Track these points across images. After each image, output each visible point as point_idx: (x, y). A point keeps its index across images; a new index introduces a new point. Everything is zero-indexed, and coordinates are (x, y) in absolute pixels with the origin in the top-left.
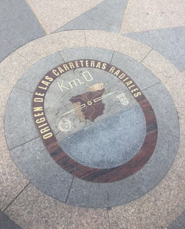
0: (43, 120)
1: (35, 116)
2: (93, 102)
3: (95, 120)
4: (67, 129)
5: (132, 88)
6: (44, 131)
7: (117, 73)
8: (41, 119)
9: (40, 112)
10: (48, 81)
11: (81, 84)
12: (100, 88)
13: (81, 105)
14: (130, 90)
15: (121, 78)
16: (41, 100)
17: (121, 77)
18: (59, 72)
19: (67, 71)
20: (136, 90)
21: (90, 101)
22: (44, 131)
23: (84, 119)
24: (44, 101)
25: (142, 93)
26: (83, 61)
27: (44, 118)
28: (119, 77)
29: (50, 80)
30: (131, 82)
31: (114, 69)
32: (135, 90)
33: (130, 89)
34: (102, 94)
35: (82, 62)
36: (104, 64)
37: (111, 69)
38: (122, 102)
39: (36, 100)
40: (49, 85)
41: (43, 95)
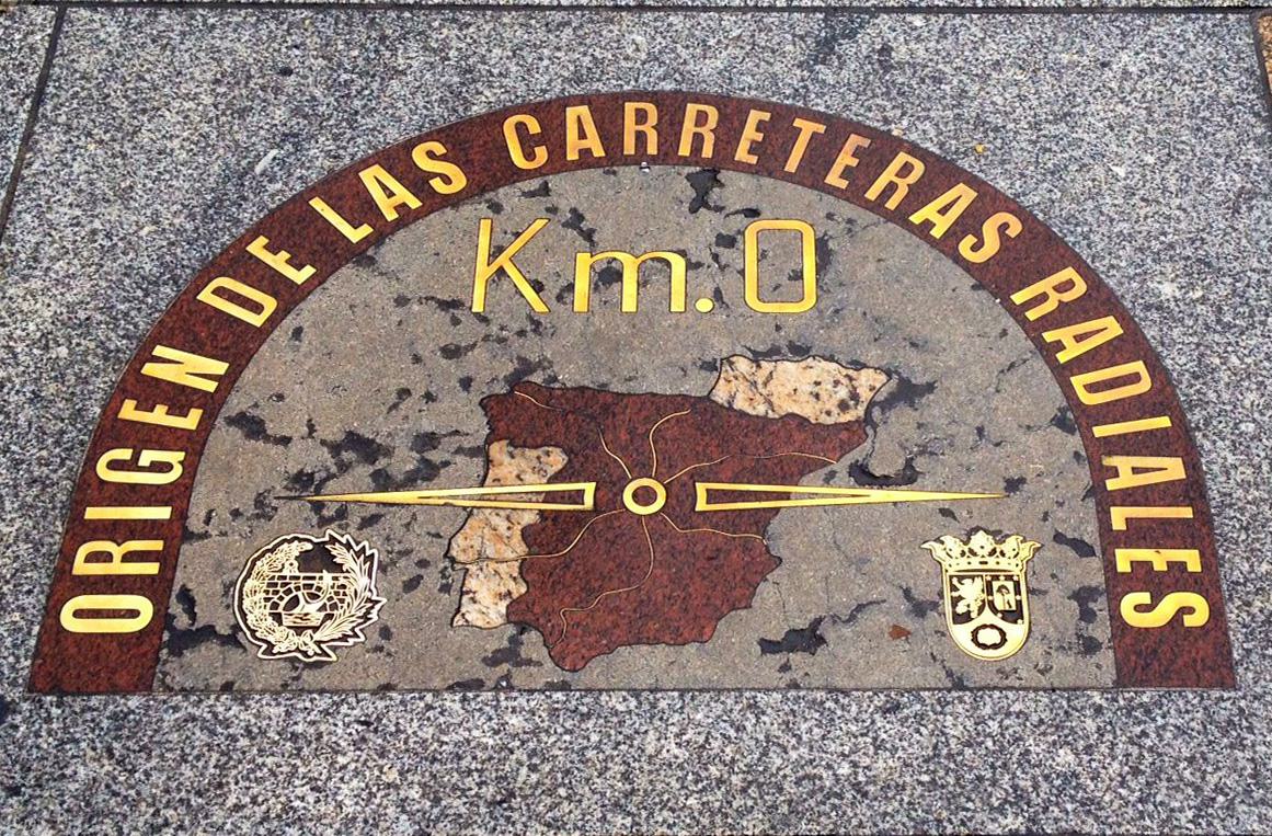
0: (164, 467)
2: (681, 498)
4: (299, 630)
5: (1139, 534)
6: (107, 557)
7: (1079, 338)
10: (418, 182)
12: (832, 405)
13: (553, 480)
14: (1112, 540)
15: (1088, 399)
16: (257, 308)
17: (1092, 388)
22: (107, 557)
23: (503, 606)
24: (274, 321)
25: (1217, 613)
26: (821, 128)
27: (181, 455)
28: (1078, 382)
29: (437, 184)
32: (1159, 559)
35: (807, 128)
38: (965, 618)
40: (406, 216)
41: (300, 276)
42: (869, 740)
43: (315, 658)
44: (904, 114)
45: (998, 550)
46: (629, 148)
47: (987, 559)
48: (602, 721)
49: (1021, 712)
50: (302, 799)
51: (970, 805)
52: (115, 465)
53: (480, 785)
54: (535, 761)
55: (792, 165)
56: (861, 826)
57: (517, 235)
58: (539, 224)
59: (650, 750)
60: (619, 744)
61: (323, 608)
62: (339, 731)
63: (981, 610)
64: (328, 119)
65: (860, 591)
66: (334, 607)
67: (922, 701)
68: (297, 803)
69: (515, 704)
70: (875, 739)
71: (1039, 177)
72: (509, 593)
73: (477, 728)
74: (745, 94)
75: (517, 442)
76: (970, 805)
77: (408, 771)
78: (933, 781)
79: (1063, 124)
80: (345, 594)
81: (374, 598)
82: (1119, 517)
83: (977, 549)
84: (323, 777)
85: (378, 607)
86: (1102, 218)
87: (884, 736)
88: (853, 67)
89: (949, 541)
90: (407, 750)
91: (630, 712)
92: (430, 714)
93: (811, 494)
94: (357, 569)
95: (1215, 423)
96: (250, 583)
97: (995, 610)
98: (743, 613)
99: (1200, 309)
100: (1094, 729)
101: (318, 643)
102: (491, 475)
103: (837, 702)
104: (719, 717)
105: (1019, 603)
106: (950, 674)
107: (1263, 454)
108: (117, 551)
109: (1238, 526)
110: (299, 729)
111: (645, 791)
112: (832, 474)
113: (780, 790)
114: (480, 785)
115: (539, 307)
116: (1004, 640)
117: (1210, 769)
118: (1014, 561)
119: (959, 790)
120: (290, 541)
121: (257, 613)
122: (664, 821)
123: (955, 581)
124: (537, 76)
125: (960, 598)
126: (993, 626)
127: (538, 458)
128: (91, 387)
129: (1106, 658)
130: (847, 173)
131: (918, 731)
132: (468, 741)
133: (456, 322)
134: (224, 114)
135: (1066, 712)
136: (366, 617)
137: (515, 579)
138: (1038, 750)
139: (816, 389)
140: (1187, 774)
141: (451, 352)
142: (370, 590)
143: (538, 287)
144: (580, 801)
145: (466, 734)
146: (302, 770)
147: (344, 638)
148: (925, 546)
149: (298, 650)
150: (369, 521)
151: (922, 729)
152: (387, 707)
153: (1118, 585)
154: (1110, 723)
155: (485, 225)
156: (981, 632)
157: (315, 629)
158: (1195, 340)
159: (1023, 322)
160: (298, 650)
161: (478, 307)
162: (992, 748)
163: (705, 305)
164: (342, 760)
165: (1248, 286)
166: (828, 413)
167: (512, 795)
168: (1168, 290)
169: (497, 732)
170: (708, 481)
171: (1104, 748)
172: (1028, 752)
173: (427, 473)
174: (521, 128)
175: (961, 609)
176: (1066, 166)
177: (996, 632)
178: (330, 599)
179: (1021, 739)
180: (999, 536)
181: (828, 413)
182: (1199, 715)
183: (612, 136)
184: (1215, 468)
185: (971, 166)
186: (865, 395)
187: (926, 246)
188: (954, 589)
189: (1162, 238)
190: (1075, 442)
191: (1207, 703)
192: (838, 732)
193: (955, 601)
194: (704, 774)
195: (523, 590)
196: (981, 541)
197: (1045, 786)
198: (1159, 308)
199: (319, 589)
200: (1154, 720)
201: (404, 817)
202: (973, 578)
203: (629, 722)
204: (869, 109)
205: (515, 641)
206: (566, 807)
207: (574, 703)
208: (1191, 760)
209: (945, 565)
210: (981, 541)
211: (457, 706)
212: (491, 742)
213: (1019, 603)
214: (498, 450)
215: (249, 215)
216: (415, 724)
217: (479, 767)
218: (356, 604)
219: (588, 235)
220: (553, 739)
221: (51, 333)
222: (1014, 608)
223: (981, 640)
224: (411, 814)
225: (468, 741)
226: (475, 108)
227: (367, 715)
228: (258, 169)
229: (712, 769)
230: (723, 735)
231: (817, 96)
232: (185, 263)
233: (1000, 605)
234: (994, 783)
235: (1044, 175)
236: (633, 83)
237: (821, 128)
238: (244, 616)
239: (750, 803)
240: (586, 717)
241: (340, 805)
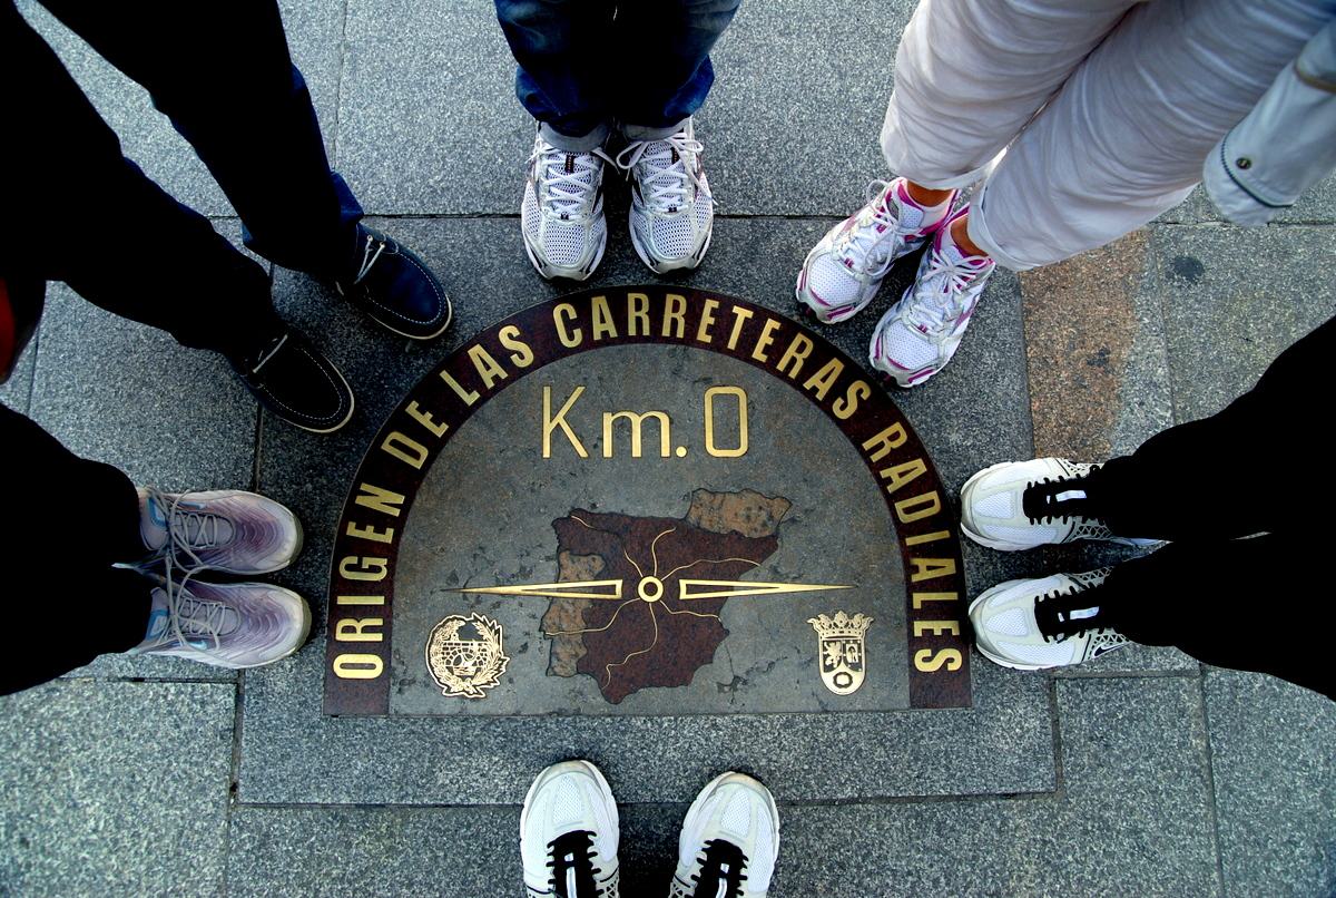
2: (671, 589)
3: (629, 703)
4: (463, 678)
5: (930, 611)
11: (665, 452)
14: (914, 615)
17: (908, 511)
21: (658, 577)
23: (574, 663)
28: (899, 506)
31: (896, 444)
33: (917, 605)
38: (829, 668)
47: (844, 629)
52: (349, 568)
55: (732, 344)
60: (642, 749)
61: (475, 664)
63: (839, 662)
66: (481, 663)
72: (577, 655)
81: (503, 657)
82: (918, 599)
83: (838, 624)
85: (505, 663)
93: (746, 588)
94: (491, 638)
96: (434, 648)
97: (846, 663)
98: (708, 666)
101: (474, 686)
102: (562, 576)
103: (760, 722)
105: (860, 658)
106: (821, 702)
108: (359, 626)
116: (851, 682)
118: (858, 631)
120: (452, 620)
121: (440, 669)
125: (828, 655)
136: (499, 670)
145: (559, 743)
147: (488, 683)
148: (810, 621)
149: (464, 691)
157: (472, 677)
159: (869, 462)
160: (464, 691)
165: (999, 435)
166: (756, 530)
171: (900, 746)
172: (861, 750)
175: (828, 662)
177: (847, 677)
178: (478, 658)
187: (813, 406)
188: (825, 649)
193: (826, 657)
195: (585, 652)
196: (840, 618)
199: (471, 651)
202: (835, 642)
209: (820, 634)
211: (553, 726)
213: (860, 658)
229: (693, 763)
231: (748, 288)
233: (850, 660)
237: (749, 314)
238: (432, 669)
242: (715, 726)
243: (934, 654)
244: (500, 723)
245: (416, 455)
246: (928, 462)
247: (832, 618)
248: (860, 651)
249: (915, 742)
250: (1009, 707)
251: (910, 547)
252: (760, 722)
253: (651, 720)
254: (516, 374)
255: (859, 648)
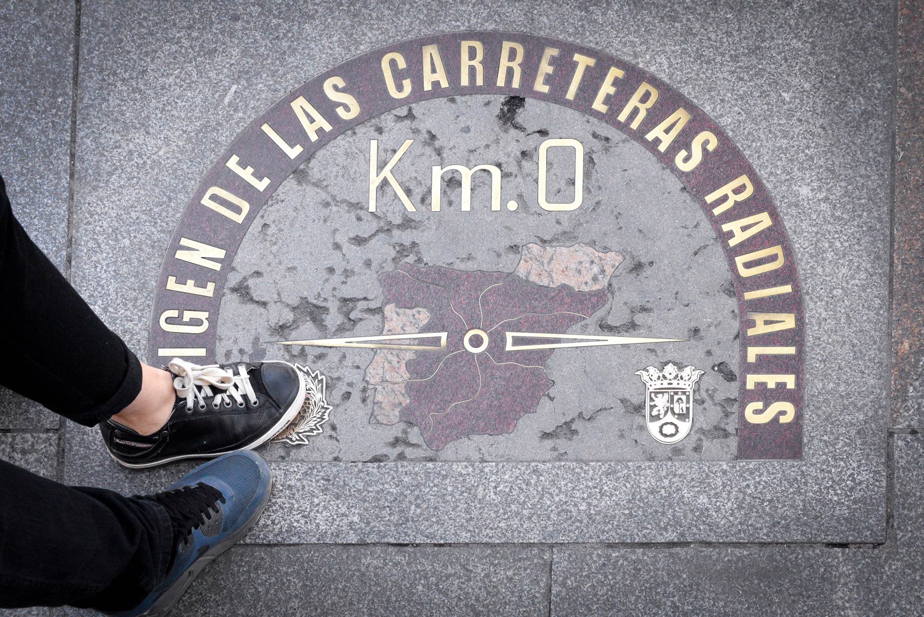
0: (197, 322)
1: (172, 284)
2: (497, 341)
8: (188, 315)
9: (200, 275)
10: (327, 109)
12: (588, 279)
15: (744, 273)
16: (238, 210)
17: (748, 265)
18: (418, 81)
19: (463, 92)
20: (781, 386)
24: (250, 218)
25: (799, 416)
26: (591, 62)
27: (206, 315)
28: (740, 260)
29: (340, 111)
30: (788, 322)
32: (771, 380)
34: (573, 320)
36: (705, 135)
37: (727, 189)
38: (657, 418)
39: (214, 198)
41: (262, 185)
42: (598, 490)
43: (297, 442)
44: (648, 49)
45: (679, 376)
46: (465, 81)
48: (453, 479)
49: (682, 474)
50: (298, 521)
51: (649, 526)
53: (390, 515)
54: (419, 502)
56: (591, 537)
57: (395, 151)
58: (408, 143)
59: (480, 496)
62: (314, 484)
63: (666, 412)
64: (266, 59)
65: (600, 402)
67: (627, 467)
68: (295, 524)
69: (406, 469)
70: (601, 490)
71: (733, 102)
73: (387, 483)
74: (542, 33)
75: (405, 304)
76: (649, 526)
77: (352, 507)
78: (630, 513)
79: (754, 57)
80: (309, 404)
81: (326, 406)
82: (753, 353)
83: (667, 375)
84: (308, 510)
85: (328, 411)
86: (770, 135)
87: (606, 488)
88: (616, 8)
89: (652, 370)
90: (350, 496)
91: (468, 474)
92: (361, 475)
95: (818, 289)
97: (674, 413)
98: (531, 415)
99: (823, 206)
100: (721, 484)
102: (386, 327)
103: (582, 468)
104: (517, 477)
105: (688, 409)
107: (843, 311)
109: (820, 359)
110: (292, 483)
111: (477, 519)
112: (586, 326)
113: (549, 518)
114: (390, 515)
115: (410, 208)
116: (677, 431)
117: (780, 506)
118: (688, 383)
119: (644, 518)
122: (487, 535)
123: (653, 395)
124: (402, 18)
125: (655, 406)
126: (672, 424)
127: (414, 315)
128: (148, 268)
129: (733, 442)
130: (608, 100)
131: (625, 485)
132: (383, 491)
133: (359, 219)
134: (199, 55)
135: (707, 474)
136: (322, 418)
137: (403, 395)
138: (689, 496)
139: (579, 267)
140: (767, 509)
141: (359, 241)
142: (323, 402)
143: (408, 192)
144: (443, 524)
145: (381, 487)
146: (296, 506)
147: (311, 430)
148: (638, 373)
150: (320, 357)
151: (627, 484)
152: (338, 471)
153: (746, 397)
154: (730, 480)
155: (374, 143)
156: (665, 427)
158: (815, 229)
161: (372, 208)
162: (664, 495)
163: (512, 205)
164: (316, 501)
166: (586, 283)
167: (407, 520)
168: (805, 191)
169: (398, 486)
170: (513, 331)
171: (724, 495)
172: (683, 497)
173: (348, 326)
174: (393, 63)
175: (655, 413)
176: (752, 93)
177: (673, 427)
179: (680, 489)
180: (680, 366)
181: (586, 283)
182: (779, 475)
183: (453, 70)
184: (814, 321)
185: (689, 93)
186: (609, 271)
188: (652, 400)
189: (807, 151)
190: (732, 303)
191: (784, 468)
192: (582, 486)
194: (508, 509)
195: (408, 401)
196: (670, 369)
197: (690, 516)
198: (797, 206)
200: (754, 479)
201: (352, 532)
202: (663, 393)
203: (468, 480)
204: (625, 44)
205: (405, 432)
206: (436, 527)
207: (438, 469)
208: (770, 501)
210: (670, 369)
211: (375, 471)
212: (395, 491)
213: (688, 409)
214: (389, 310)
215: (225, 137)
216: (354, 481)
217: (389, 505)
218: (316, 410)
219: (439, 152)
220: (428, 490)
221: (118, 228)
222: (685, 412)
223: (664, 432)
224: (355, 530)
225: (383, 491)
226: (362, 47)
227: (328, 476)
228: (227, 100)
229: (513, 506)
230: (519, 488)
232: (190, 176)
233: (677, 411)
234: (663, 514)
235: (736, 100)
236: (466, 24)
239: (533, 525)
240: (445, 477)
241: (318, 525)
242: (535, 471)
243: (766, 406)
244: (323, 467)
245: (238, 210)
246: (774, 215)
247: (661, 370)
248: (688, 402)
249: (740, 491)
250: (842, 459)
251: (747, 302)
252: (582, 468)
253: (472, 466)
254: (342, 127)
255: (688, 397)
